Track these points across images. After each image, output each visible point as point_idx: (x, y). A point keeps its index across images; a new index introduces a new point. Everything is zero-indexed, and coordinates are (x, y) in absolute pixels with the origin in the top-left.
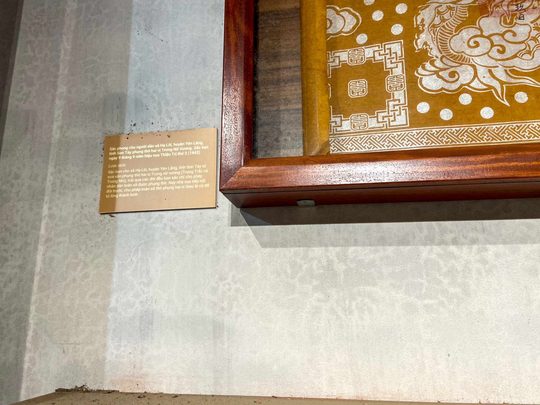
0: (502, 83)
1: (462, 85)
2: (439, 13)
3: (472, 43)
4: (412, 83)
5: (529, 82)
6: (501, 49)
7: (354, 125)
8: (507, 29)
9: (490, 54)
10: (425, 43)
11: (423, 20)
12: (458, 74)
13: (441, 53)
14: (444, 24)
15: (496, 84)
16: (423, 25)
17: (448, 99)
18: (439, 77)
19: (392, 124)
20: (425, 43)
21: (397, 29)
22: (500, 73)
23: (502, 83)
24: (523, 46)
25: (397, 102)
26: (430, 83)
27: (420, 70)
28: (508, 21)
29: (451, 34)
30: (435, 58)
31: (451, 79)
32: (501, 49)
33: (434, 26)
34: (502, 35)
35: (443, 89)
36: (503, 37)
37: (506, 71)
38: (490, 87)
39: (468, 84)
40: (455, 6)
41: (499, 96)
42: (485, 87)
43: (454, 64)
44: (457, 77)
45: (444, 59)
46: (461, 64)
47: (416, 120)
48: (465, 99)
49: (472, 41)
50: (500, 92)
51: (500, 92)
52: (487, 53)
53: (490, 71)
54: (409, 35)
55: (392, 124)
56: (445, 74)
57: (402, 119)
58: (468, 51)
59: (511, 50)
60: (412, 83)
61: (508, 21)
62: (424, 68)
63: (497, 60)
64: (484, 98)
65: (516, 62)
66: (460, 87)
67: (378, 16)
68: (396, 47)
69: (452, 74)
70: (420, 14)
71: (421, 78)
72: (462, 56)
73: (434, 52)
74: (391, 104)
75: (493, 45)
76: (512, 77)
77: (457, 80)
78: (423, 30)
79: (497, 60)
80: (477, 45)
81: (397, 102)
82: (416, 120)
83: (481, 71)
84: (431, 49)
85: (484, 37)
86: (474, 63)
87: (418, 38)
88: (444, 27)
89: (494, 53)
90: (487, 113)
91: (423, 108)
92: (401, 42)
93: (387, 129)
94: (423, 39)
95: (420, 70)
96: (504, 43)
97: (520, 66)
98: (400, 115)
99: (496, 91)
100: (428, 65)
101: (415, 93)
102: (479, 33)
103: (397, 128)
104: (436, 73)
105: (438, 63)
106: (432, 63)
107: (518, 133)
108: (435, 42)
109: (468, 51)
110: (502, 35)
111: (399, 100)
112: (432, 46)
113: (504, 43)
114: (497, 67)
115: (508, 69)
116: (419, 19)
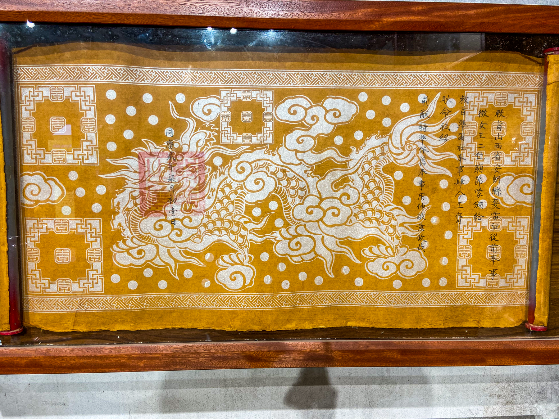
0: (176, 261)
1: (147, 261)
2: (133, 197)
3: (157, 227)
4: (108, 256)
5: (195, 261)
6: (179, 233)
7: (60, 288)
8: (186, 215)
9: (170, 236)
10: (120, 224)
11: (119, 203)
12: (144, 252)
13: (132, 234)
14: (136, 208)
15: (171, 261)
16: (119, 208)
17: (134, 273)
18: (129, 254)
19: (90, 290)
20: (120, 224)
21: (97, 208)
22: (175, 253)
23: (176, 261)
24: (195, 231)
25: (95, 272)
26: (123, 260)
27: (115, 246)
28: (188, 208)
29: (141, 217)
30: (127, 238)
31: (140, 256)
32: (179, 233)
33: (128, 210)
34: (181, 220)
35: (131, 264)
36: (182, 223)
37: (180, 251)
38: (167, 264)
39: (151, 261)
40: (147, 192)
41: (173, 273)
42: (162, 264)
43: (143, 244)
44: (143, 253)
45: (134, 240)
46: (147, 244)
47: (110, 289)
48: (148, 273)
49: (158, 224)
50: (173, 269)
51: (173, 269)
52: (168, 235)
53: (168, 251)
54: (108, 214)
55: (90, 290)
56: (134, 252)
57: (99, 287)
58: (153, 232)
59: (187, 233)
60: (108, 256)
61: (188, 208)
62: (118, 246)
63: (174, 242)
64: (161, 272)
65: (189, 244)
66: (145, 263)
67: (81, 192)
68: (96, 223)
69: (139, 252)
70: (116, 197)
71: (115, 255)
72: (149, 236)
73: (127, 233)
74: (91, 273)
75: (173, 229)
76: (183, 256)
77: (144, 256)
78: (118, 213)
79: (174, 242)
80: (161, 227)
81: (95, 272)
82: (110, 289)
83: (163, 250)
84: (124, 230)
85: (167, 221)
86: (157, 243)
87: (114, 219)
88: (135, 210)
89: (173, 236)
90: (163, 284)
91: (116, 278)
92: (100, 220)
93: (86, 294)
94: (120, 220)
95: (115, 246)
96: (182, 228)
97: (191, 248)
98: (97, 283)
99: (171, 267)
100: (121, 244)
101: (109, 268)
102: (164, 218)
103: (95, 294)
104: (127, 251)
105: (129, 242)
106: (124, 242)
107: (182, 301)
108: (128, 224)
109: (153, 232)
110: (181, 220)
111: (97, 270)
112: (125, 227)
113: (182, 228)
114: (174, 247)
115: (182, 250)
116: (116, 201)
